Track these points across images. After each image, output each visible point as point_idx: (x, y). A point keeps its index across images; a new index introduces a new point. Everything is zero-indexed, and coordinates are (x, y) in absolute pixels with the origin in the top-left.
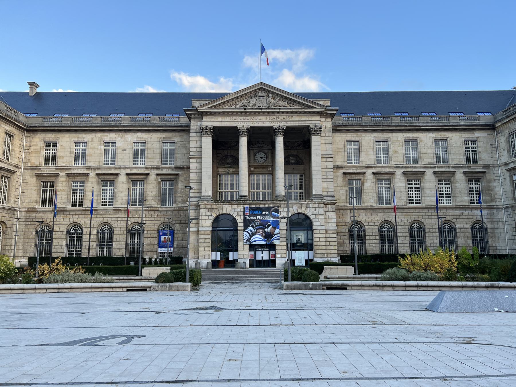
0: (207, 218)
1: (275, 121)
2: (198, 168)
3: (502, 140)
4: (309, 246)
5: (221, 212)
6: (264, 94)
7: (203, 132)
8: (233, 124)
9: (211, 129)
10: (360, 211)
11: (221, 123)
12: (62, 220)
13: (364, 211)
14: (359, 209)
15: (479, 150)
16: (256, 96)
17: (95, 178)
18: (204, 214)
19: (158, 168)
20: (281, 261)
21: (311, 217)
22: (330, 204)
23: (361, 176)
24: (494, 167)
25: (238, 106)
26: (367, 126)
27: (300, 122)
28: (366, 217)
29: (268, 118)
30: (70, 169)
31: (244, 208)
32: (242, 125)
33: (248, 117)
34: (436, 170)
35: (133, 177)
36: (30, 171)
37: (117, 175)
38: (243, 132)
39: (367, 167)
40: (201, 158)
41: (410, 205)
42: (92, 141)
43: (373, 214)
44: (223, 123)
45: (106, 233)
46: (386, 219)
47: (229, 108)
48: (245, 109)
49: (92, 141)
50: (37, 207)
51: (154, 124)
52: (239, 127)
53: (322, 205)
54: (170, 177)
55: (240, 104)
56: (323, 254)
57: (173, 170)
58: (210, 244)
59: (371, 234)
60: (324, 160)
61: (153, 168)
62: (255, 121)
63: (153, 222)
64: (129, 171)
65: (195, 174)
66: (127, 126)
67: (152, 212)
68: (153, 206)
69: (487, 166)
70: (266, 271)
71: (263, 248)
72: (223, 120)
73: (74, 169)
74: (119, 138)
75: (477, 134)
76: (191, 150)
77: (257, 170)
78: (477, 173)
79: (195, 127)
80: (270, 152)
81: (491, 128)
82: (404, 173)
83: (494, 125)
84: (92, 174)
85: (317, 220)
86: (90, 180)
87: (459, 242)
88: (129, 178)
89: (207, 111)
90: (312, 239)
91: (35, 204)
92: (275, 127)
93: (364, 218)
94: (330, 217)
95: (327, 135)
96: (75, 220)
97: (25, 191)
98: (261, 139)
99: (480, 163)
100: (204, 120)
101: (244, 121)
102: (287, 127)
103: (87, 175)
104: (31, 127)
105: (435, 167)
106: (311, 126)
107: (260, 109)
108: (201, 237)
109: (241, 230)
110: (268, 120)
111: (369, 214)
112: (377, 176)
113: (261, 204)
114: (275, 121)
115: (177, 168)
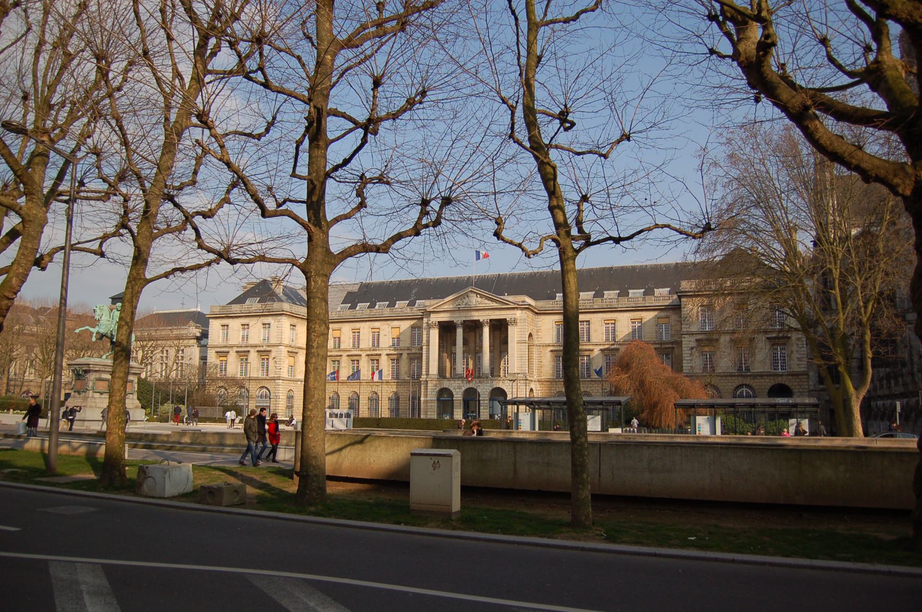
45: (374, 400)
84: (364, 354)
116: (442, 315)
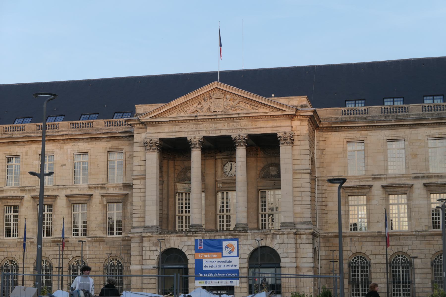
0: (151, 253)
1: (235, 129)
2: (142, 190)
5: (168, 247)
6: (221, 95)
7: (147, 146)
8: (183, 135)
9: (156, 143)
10: (364, 239)
11: (168, 134)
16: (211, 98)
17: (30, 202)
18: (148, 249)
19: (103, 187)
21: (279, 252)
22: (305, 234)
23: (366, 190)
25: (189, 112)
27: (265, 129)
28: (372, 248)
29: (226, 125)
31: (196, 241)
32: (193, 136)
33: (201, 126)
35: (74, 199)
37: (56, 197)
38: (195, 144)
39: (374, 179)
40: (145, 179)
41: (435, 230)
42: (26, 155)
44: (171, 134)
46: (400, 250)
47: (179, 115)
48: (196, 116)
49: (26, 155)
51: (98, 129)
52: (189, 139)
53: (292, 236)
54: (117, 198)
55: (192, 109)
57: (120, 189)
59: (378, 270)
60: (298, 176)
61: (97, 187)
62: (209, 130)
63: (98, 256)
64: (69, 193)
66: (66, 135)
67: (97, 244)
68: (98, 236)
71: (219, 290)
72: (171, 130)
74: (57, 150)
76: (135, 168)
77: (227, 185)
79: (139, 140)
82: (425, 185)
85: (285, 255)
88: (70, 201)
89: (151, 120)
92: (233, 137)
93: (369, 248)
94: (305, 250)
95: (302, 143)
96: (9, 254)
100: (148, 131)
101: (196, 131)
103: (22, 198)
106: (279, 134)
107: (214, 115)
109: (192, 268)
110: (226, 127)
111: (377, 244)
112: (388, 190)
113: (215, 235)
114: (235, 129)
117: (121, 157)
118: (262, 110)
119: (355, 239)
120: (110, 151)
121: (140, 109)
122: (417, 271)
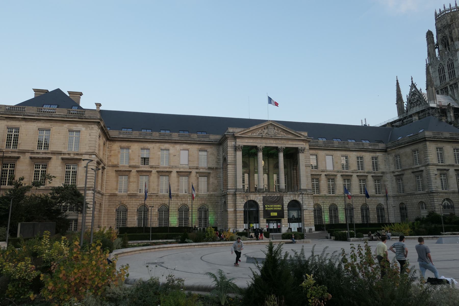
3: (391, 158)
4: (299, 220)
5: (249, 199)
10: (319, 198)
12: (134, 202)
13: (321, 198)
14: (318, 196)
15: (379, 163)
18: (239, 200)
19: (197, 168)
20: (284, 230)
24: (387, 173)
26: (321, 147)
30: (139, 167)
31: (263, 197)
34: (358, 174)
36: (111, 168)
37: (171, 172)
39: (322, 171)
42: (153, 148)
43: (326, 200)
49: (153, 148)
50: (116, 193)
51: (194, 139)
53: (307, 195)
56: (308, 224)
58: (243, 219)
64: (178, 170)
65: (231, 175)
66: (178, 140)
69: (383, 173)
70: (277, 235)
73: (141, 167)
75: (378, 154)
78: (379, 176)
79: (231, 145)
80: (267, 160)
81: (385, 151)
82: (342, 175)
83: (386, 150)
84: (154, 171)
86: (153, 175)
87: (371, 216)
90: (301, 216)
91: (115, 191)
97: (108, 181)
98: (271, 154)
99: (380, 171)
102: (286, 148)
104: (113, 138)
105: (357, 172)
108: (238, 214)
115: (209, 168)
116: (246, 140)
117: (205, 153)
118: (290, 136)
119: (315, 198)
120: (201, 150)
121: (231, 130)
122: (339, 212)
